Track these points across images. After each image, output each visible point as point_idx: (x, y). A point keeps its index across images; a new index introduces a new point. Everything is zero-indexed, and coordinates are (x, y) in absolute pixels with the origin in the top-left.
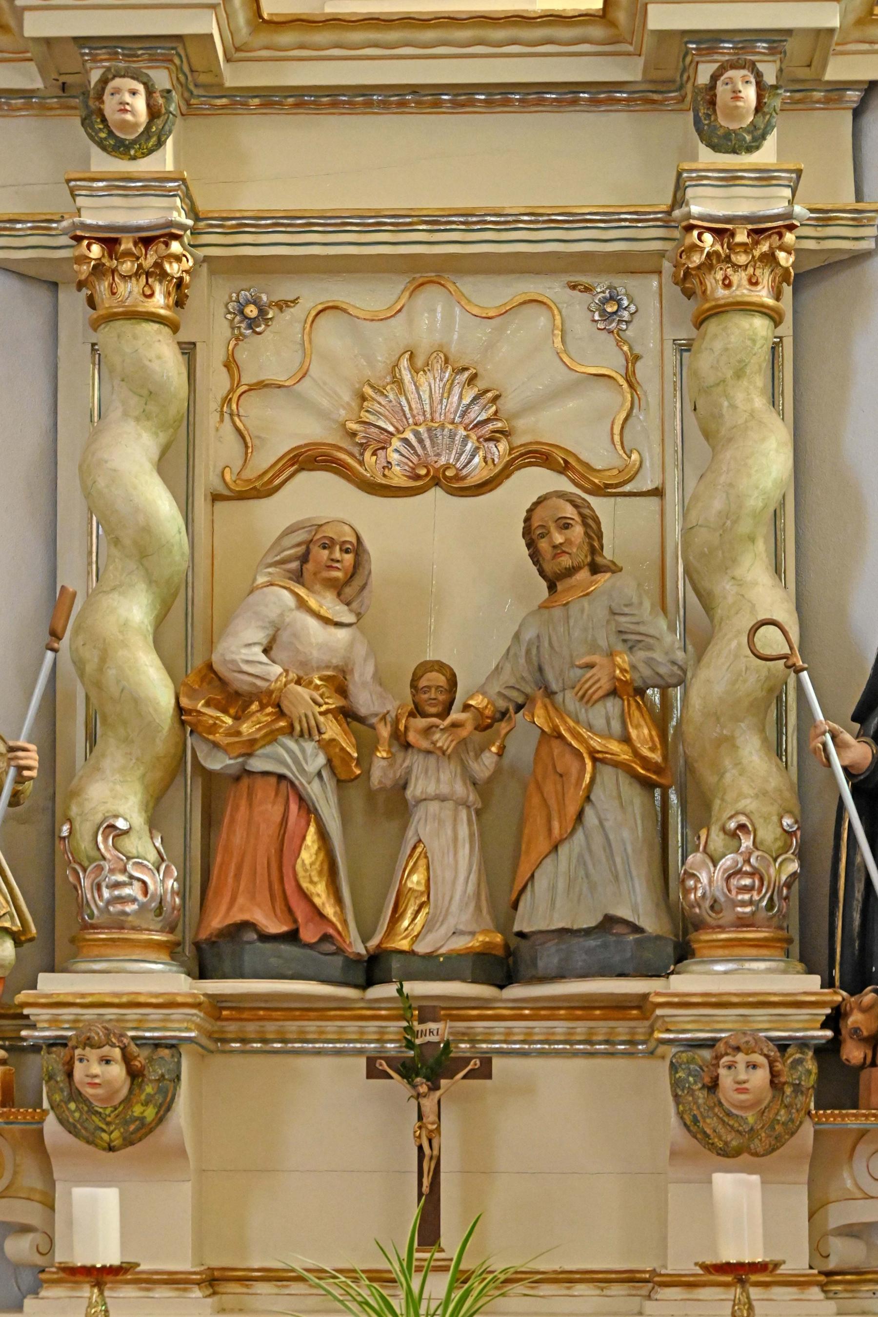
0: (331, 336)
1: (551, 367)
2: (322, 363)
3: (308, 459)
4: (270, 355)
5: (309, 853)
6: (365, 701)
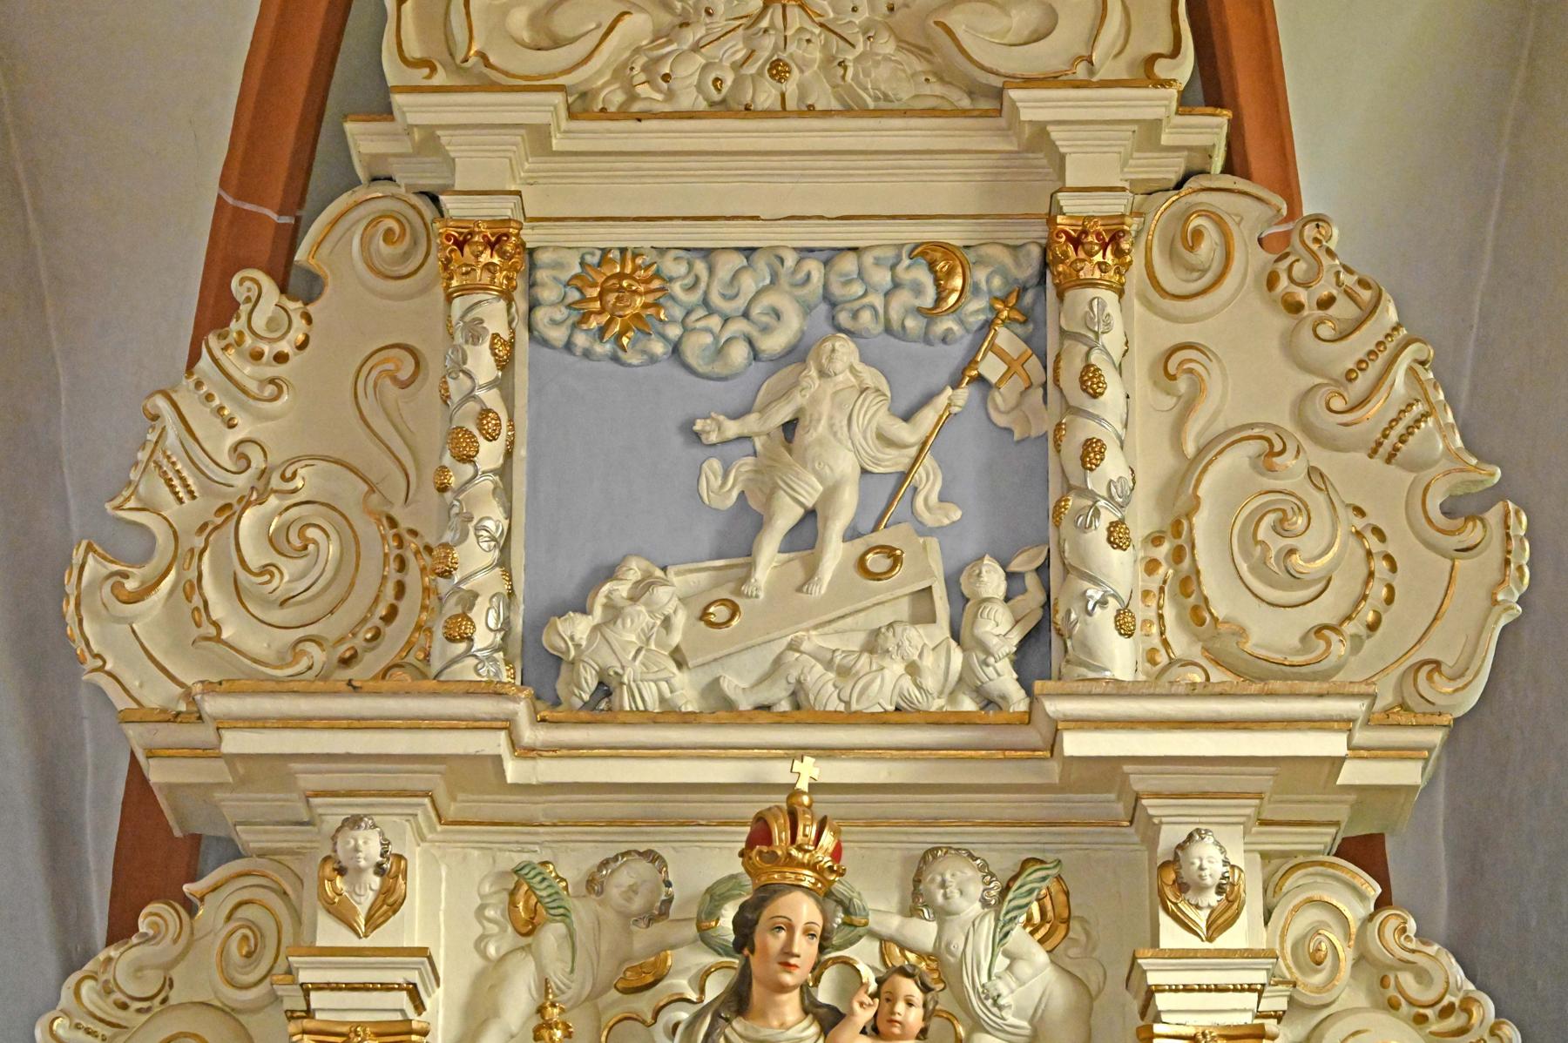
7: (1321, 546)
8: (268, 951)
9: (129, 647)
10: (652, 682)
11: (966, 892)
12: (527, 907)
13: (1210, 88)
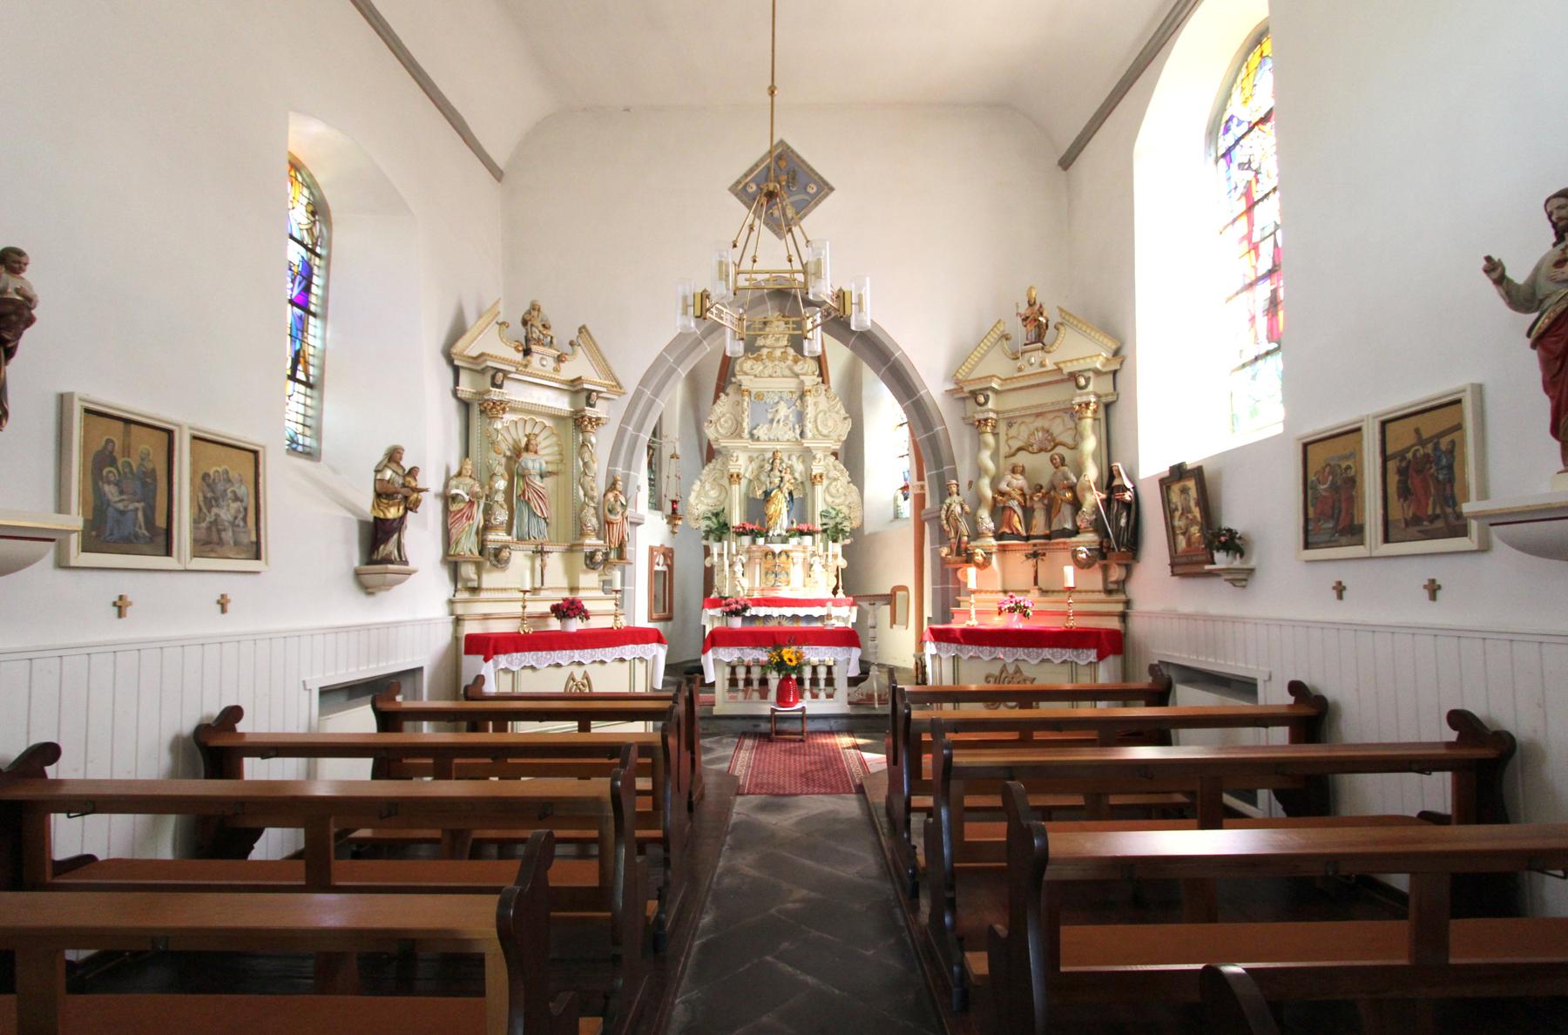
0: (1023, 428)
1: (1060, 429)
2: (1022, 433)
3: (1020, 449)
4: (1013, 432)
5: (1016, 519)
6: (1027, 491)
7: (830, 423)
8: (725, 464)
9: (710, 433)
10: (763, 437)
11: (794, 458)
12: (751, 460)
13: (821, 374)
